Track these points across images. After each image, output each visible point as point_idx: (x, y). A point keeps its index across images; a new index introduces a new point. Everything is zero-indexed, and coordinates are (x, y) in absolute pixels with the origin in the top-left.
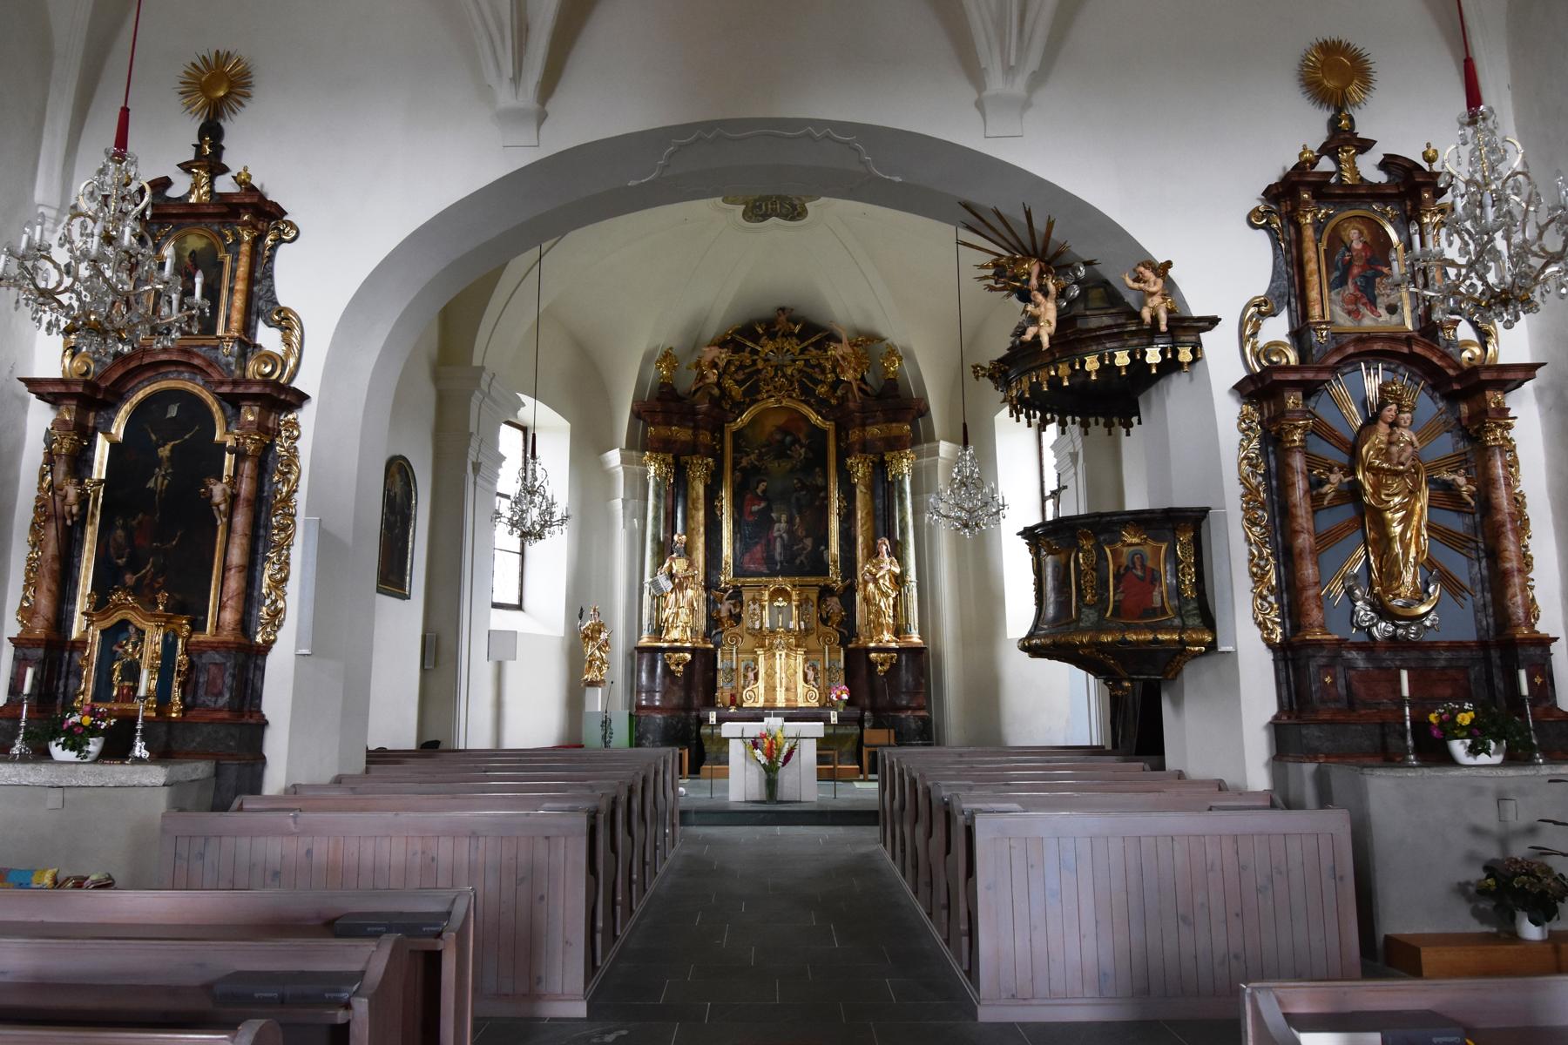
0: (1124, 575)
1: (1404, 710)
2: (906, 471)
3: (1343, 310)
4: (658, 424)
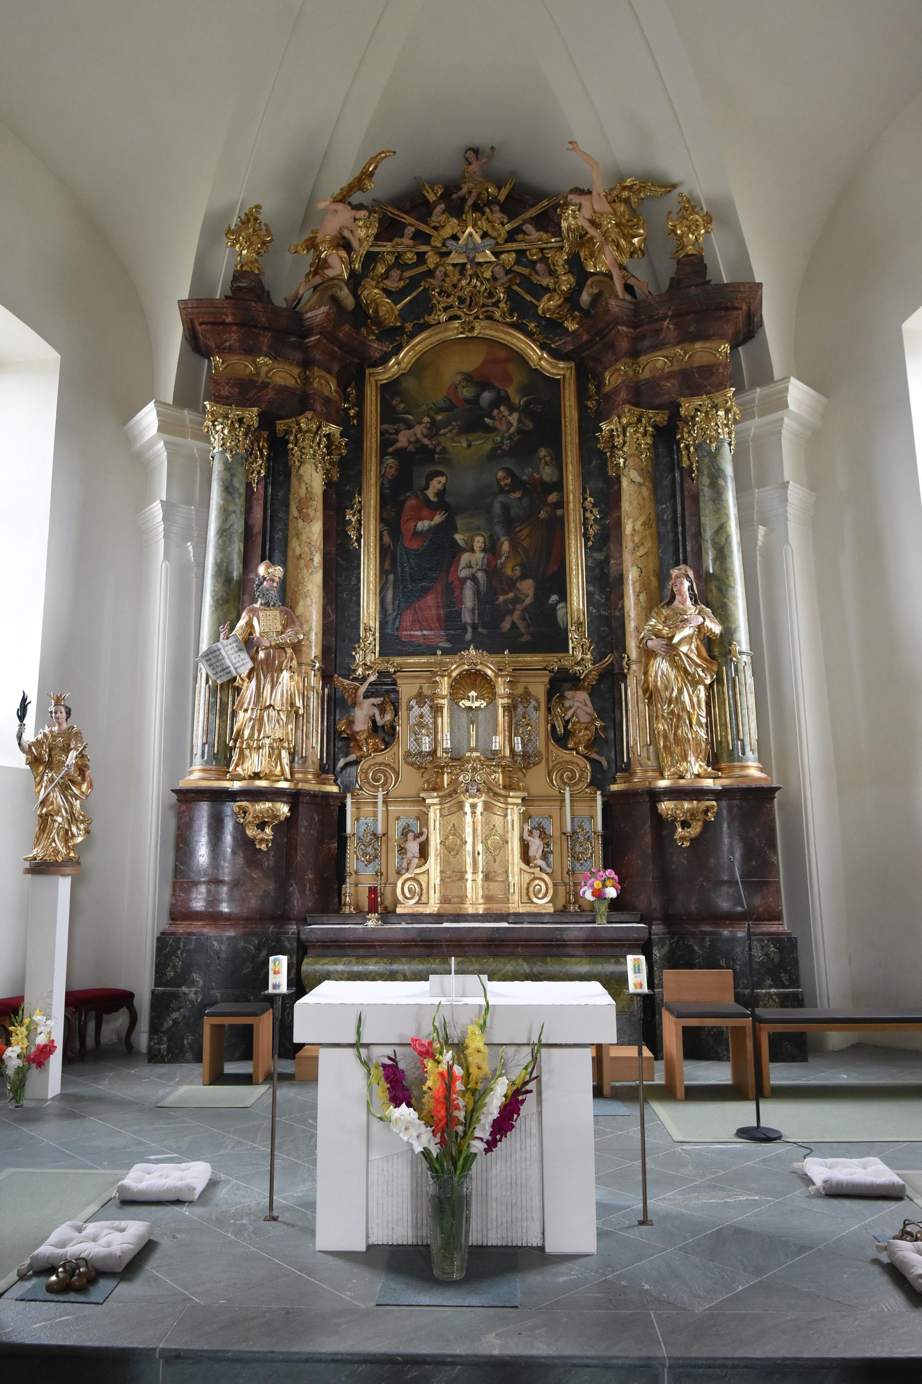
4: (231, 350)
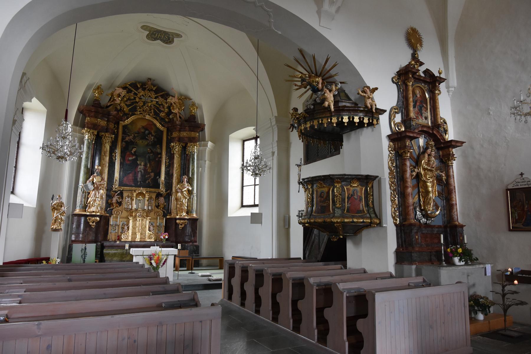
1: (442, 248)
2: (196, 151)
4: (92, 117)
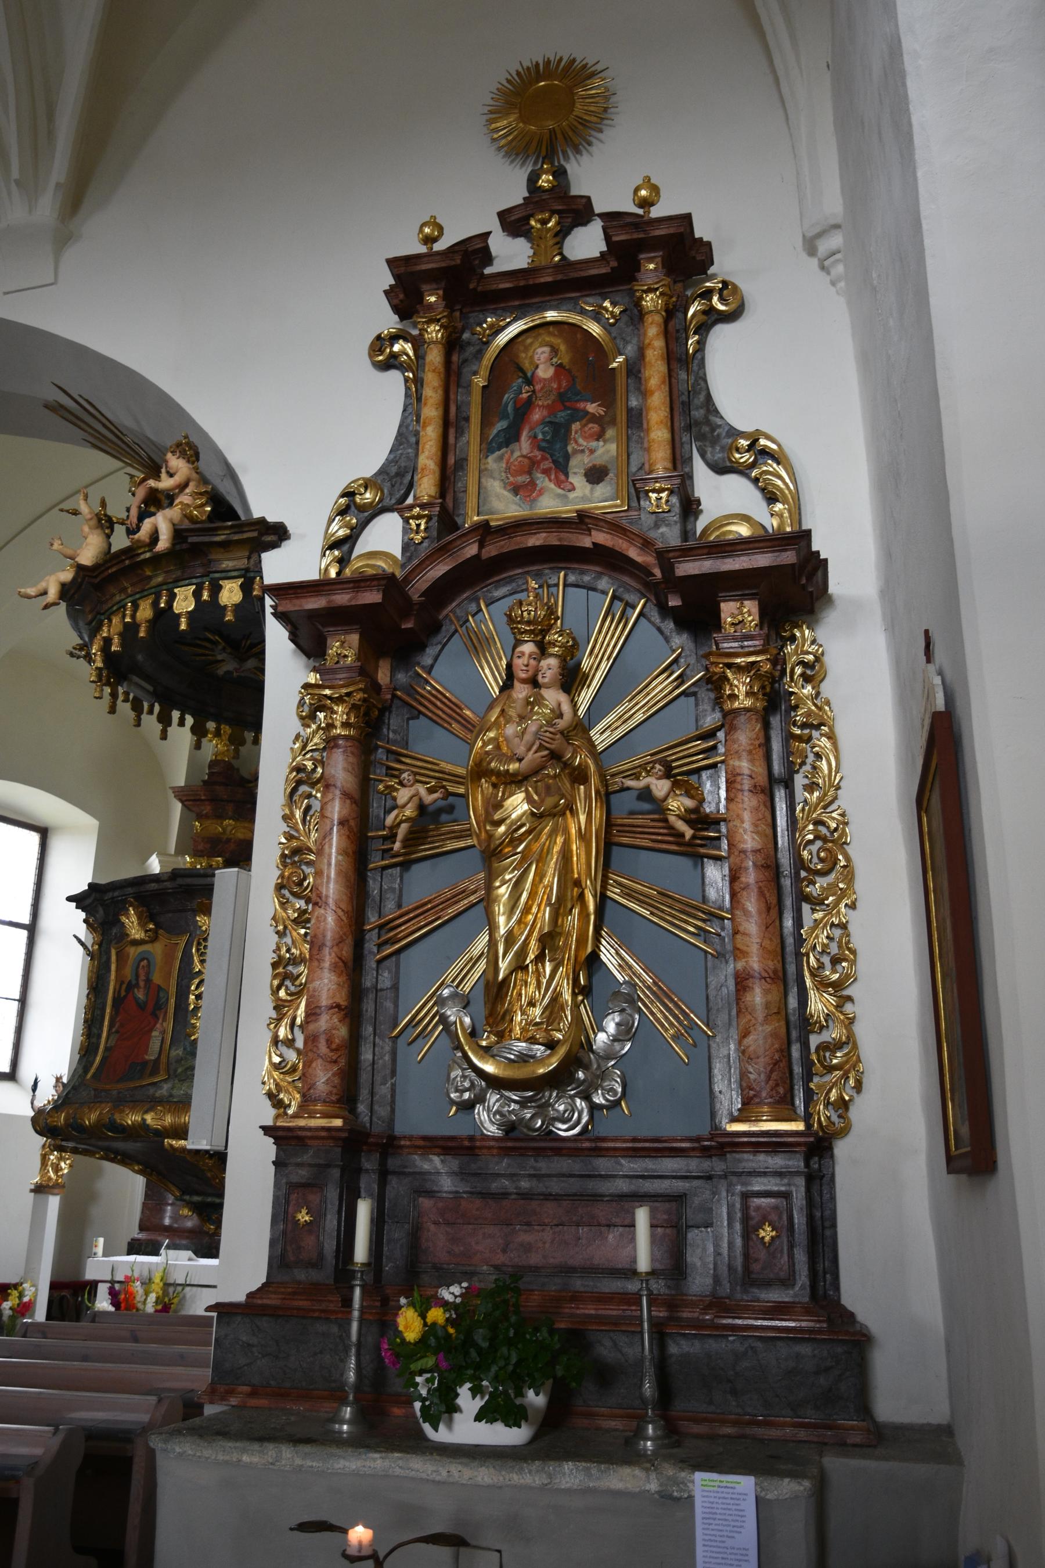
0: (125, 996)
3: (505, 485)
4: (207, 817)
